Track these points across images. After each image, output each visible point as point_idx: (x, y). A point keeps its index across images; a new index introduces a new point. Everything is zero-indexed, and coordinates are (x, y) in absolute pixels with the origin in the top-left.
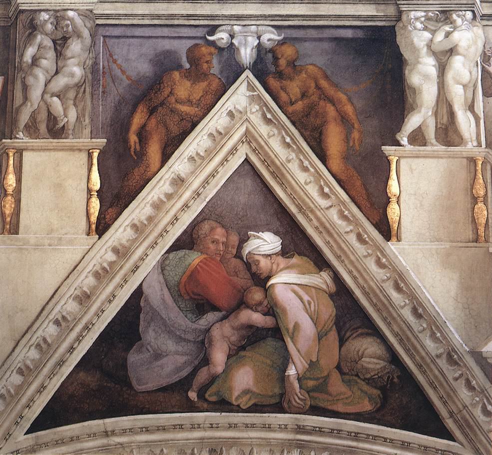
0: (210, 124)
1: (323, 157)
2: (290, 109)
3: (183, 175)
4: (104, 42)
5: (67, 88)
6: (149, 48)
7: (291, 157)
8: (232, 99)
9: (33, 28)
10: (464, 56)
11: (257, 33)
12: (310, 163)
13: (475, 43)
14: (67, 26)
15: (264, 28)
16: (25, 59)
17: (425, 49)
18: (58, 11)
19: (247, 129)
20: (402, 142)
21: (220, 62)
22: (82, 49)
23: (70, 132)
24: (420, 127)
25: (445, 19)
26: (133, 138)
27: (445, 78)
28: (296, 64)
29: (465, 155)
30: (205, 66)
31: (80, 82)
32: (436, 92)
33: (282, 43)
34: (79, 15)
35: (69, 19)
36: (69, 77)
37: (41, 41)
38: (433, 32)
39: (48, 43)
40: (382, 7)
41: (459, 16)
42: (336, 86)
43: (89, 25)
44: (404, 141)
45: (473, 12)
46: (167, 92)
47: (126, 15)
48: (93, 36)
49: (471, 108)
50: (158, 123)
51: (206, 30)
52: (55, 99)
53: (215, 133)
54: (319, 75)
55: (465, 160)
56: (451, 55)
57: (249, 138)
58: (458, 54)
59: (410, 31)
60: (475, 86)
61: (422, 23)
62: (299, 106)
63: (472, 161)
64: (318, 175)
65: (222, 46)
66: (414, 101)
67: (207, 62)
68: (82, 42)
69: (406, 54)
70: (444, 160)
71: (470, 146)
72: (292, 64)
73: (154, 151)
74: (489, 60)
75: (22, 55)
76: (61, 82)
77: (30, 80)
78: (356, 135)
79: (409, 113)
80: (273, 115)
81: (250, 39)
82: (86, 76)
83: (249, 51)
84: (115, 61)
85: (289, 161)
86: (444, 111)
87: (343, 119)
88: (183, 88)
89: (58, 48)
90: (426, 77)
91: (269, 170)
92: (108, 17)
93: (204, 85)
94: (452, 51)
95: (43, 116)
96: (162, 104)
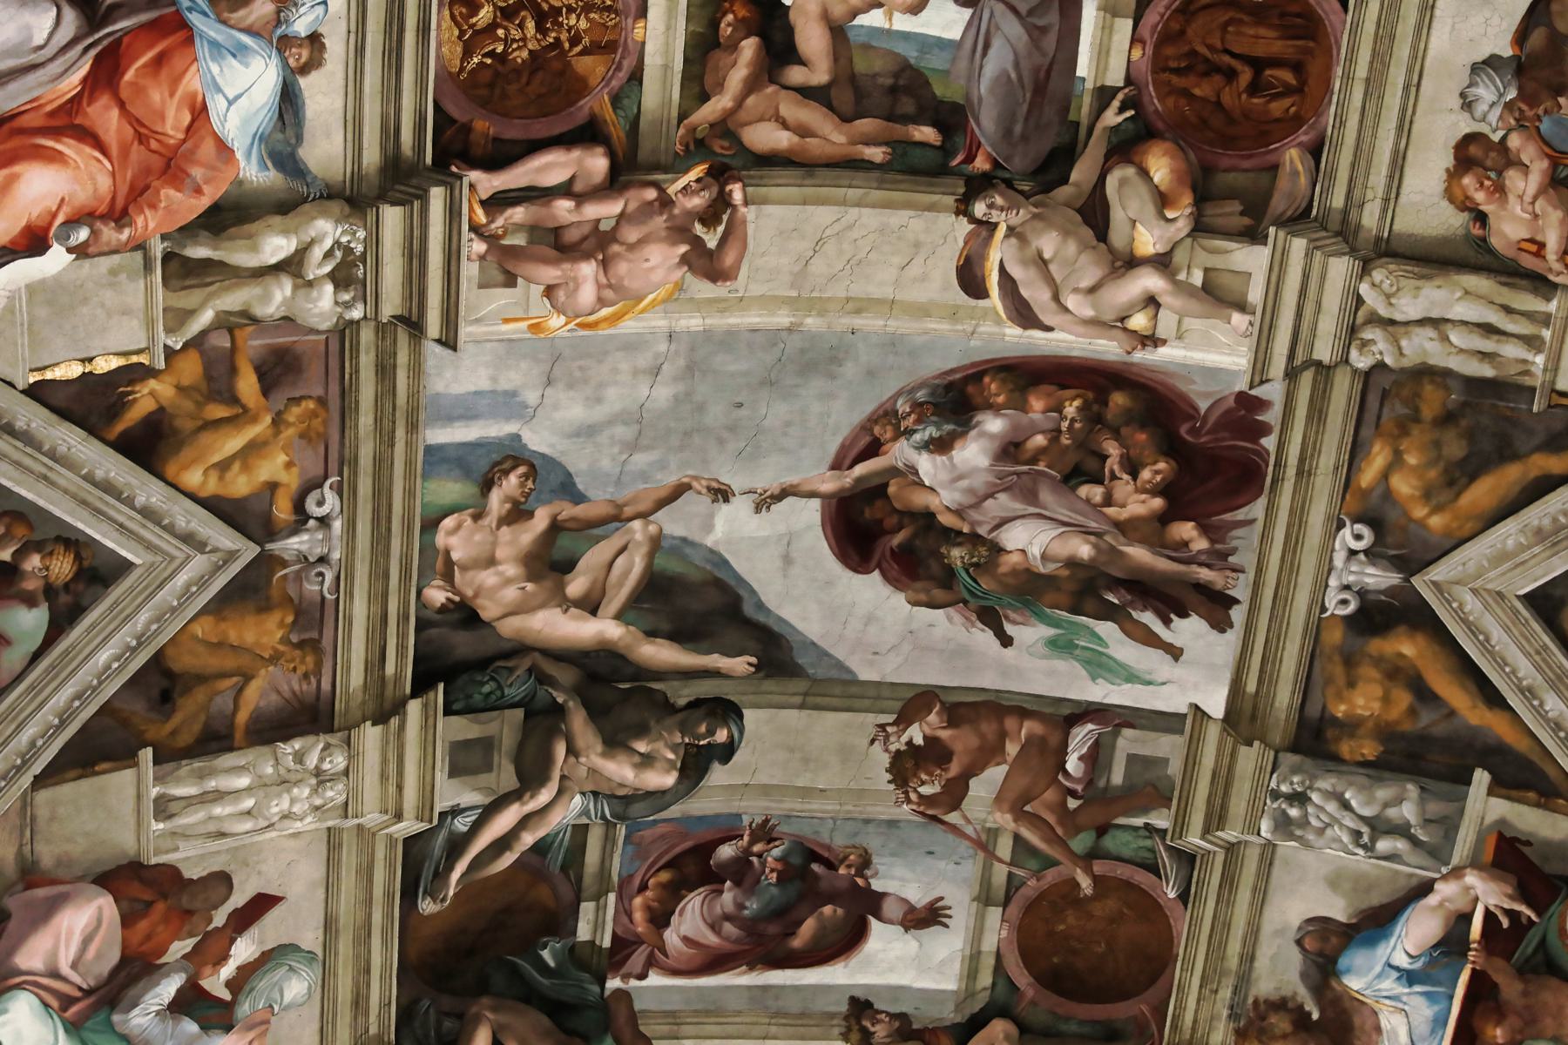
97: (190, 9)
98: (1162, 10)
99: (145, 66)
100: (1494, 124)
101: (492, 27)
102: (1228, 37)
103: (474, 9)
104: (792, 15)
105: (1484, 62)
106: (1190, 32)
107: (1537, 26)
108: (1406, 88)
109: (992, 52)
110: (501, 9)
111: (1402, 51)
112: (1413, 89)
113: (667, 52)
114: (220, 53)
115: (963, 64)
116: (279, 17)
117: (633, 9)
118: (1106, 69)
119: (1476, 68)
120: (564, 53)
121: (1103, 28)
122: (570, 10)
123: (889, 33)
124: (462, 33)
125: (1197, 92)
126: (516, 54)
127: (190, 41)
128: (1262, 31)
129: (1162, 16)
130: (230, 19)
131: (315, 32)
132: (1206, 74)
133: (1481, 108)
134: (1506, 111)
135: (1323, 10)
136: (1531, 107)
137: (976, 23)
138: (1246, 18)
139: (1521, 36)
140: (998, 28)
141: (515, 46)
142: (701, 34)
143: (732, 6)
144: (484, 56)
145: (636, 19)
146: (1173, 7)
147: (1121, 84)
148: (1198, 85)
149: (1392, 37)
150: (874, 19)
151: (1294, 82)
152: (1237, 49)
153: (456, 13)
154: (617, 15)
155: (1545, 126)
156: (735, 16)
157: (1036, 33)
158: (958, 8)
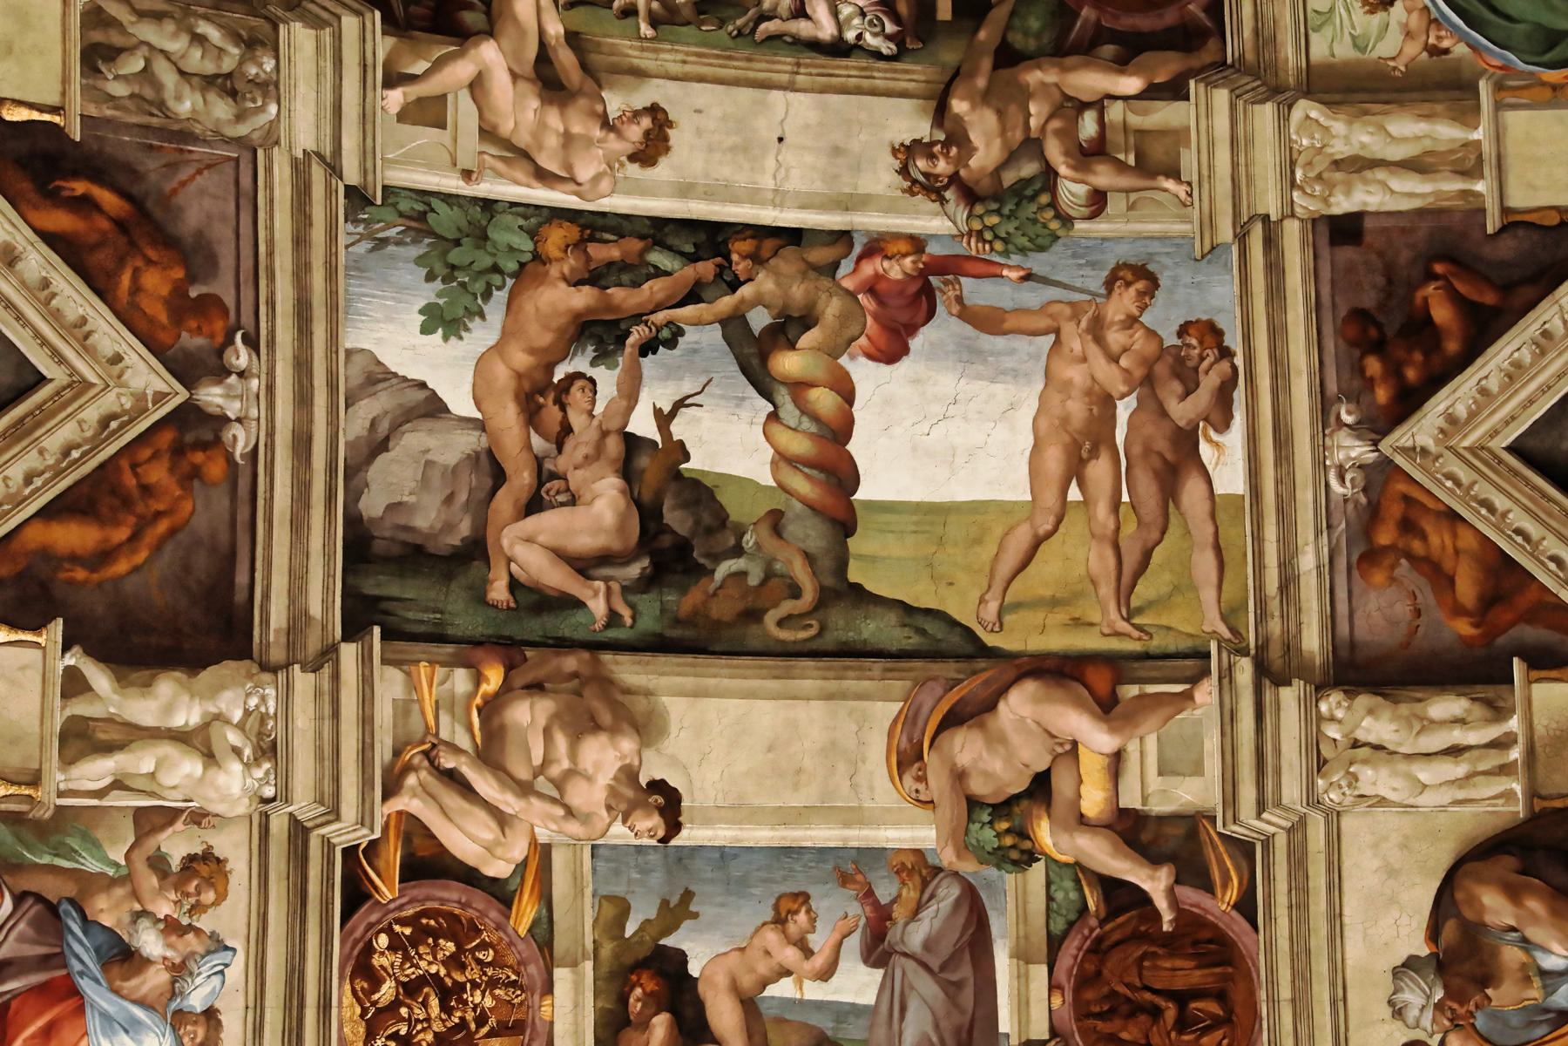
0: (102, 322)
1: (48, 513)
2: (124, 463)
3: (20, 266)
4: (229, 159)
5: (158, 86)
6: (222, 234)
7: (47, 457)
8: (142, 364)
9: (251, 44)
10: (202, 779)
11: (246, 417)
12: (38, 489)
13: (224, 798)
14: (254, 100)
15: (254, 430)
16: (201, 22)
17: (213, 710)
18: (277, 87)
19: (92, 385)
20: (68, 655)
21: (200, 349)
22: (218, 120)
23: (91, 82)
24: (90, 689)
25: (261, 748)
26: (80, 187)
27: (166, 741)
28: (196, 483)
29: (45, 767)
30: (193, 324)
31: (168, 109)
32: (144, 724)
33: (229, 458)
34: (271, 122)
35: (264, 105)
36: (176, 91)
37: (229, 54)
38: (241, 727)
39: (228, 65)
40: (283, 640)
41: (267, 773)
42: (158, 548)
43: (255, 136)
44: (70, 660)
45: (274, 799)
46: (152, 254)
47: (272, 201)
48: (239, 141)
49: (118, 785)
50: (104, 233)
51: (251, 330)
52: (141, 64)
53: (87, 328)
54: (178, 518)
55: (37, 767)
56: (204, 755)
57: (79, 387)
58: (205, 768)
59: (243, 685)
60: (152, 794)
61: (257, 707)
62: (130, 481)
63: (35, 780)
64: (19, 502)
65: (225, 356)
66: (132, 684)
67: (199, 328)
68: (229, 121)
69: (208, 675)
70: (37, 729)
71: (60, 777)
72: (196, 473)
73: (61, 220)
74: (195, 823)
75: (206, 18)
76: (169, 78)
77: (170, 26)
78: (80, 574)
79: (113, 671)
80: (115, 432)
81: (237, 405)
82: (178, 121)
83: (219, 401)
84: (199, 172)
85: (41, 452)
86: (113, 735)
87: (105, 555)
88: (157, 282)
89: (220, 80)
90: (169, 709)
91: (26, 416)
92: (269, 170)
93: (163, 317)
94: (210, 757)
95: (116, 39)
96: (132, 244)
97: (81, 974)
98: (1074, 952)
99: (33, 1037)
100: (1429, 1029)
101: (395, 1005)
102: (1145, 973)
103: (376, 983)
104: (701, 988)
105: (1403, 965)
106: (1105, 972)
107: (1446, 919)
108: (1334, 1003)
109: (909, 1015)
110: (404, 985)
111: (1321, 966)
112: (1341, 1004)
113: (576, 1032)
114: (112, 1028)
115: (881, 1032)
116: (173, 988)
117: (539, 984)
118: (1028, 1022)
119: (1397, 973)
120: (470, 1035)
121: (1019, 977)
122: (475, 985)
123: (802, 1003)
124: (364, 1011)
125: (1125, 1035)
126: (421, 1036)
127: (80, 1010)
128: (1179, 963)
129: (1076, 958)
130: (123, 988)
131: (211, 1007)
132: (1131, 1015)
133: (1412, 1014)
134: (1437, 1013)
135: (1233, 932)
136: (1461, 1004)
137: (888, 984)
138: (1160, 951)
139: (1434, 933)
140: (912, 988)
141: (419, 1027)
142: (610, 1011)
143: (639, 980)
144: (389, 1038)
145: (543, 995)
146: (1085, 947)
147: (1046, 1037)
148: (1124, 1028)
149: (1308, 952)
150: (783, 989)
151: (1221, 1013)
152: (1157, 986)
153: (358, 988)
154: (523, 991)
155: (1480, 1021)
156: (643, 989)
157: (952, 989)
158: (870, 969)
